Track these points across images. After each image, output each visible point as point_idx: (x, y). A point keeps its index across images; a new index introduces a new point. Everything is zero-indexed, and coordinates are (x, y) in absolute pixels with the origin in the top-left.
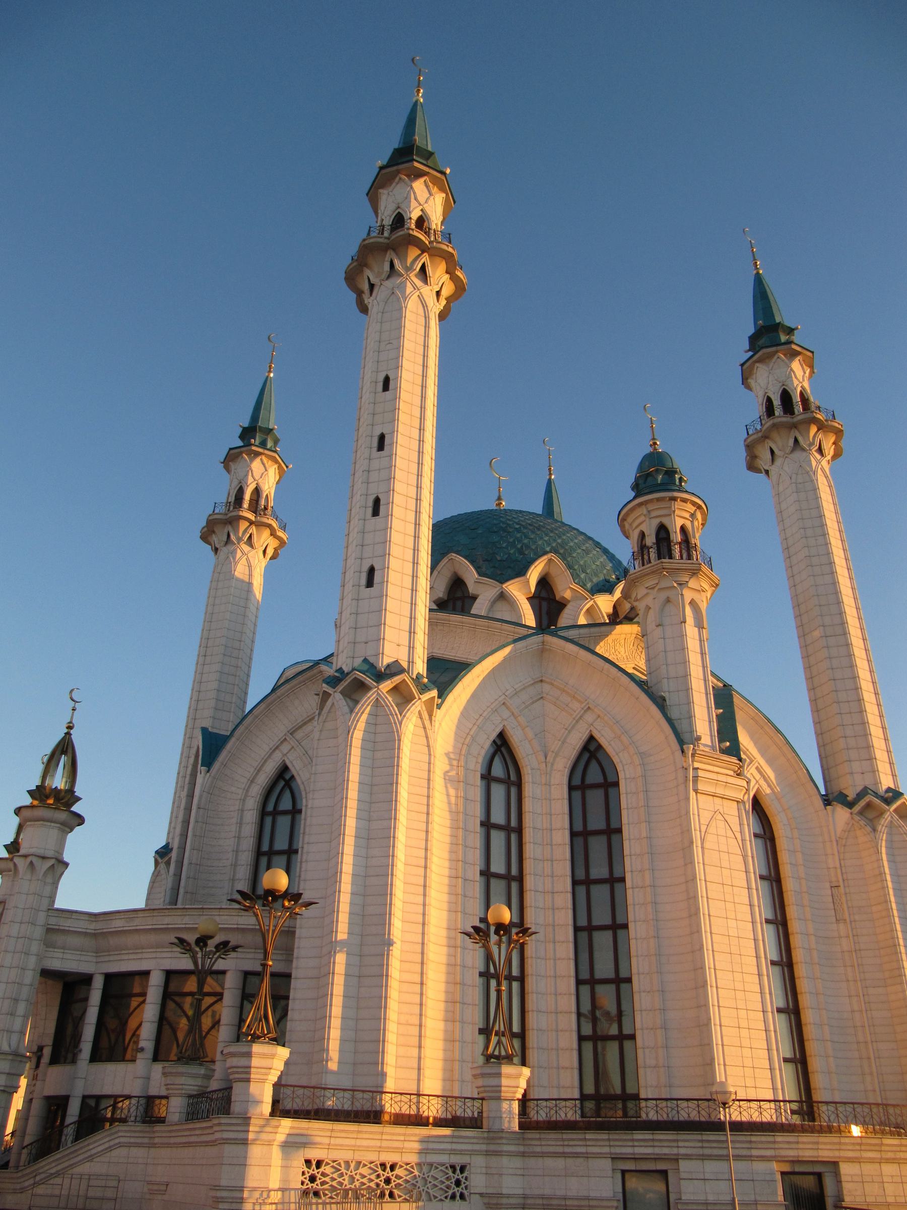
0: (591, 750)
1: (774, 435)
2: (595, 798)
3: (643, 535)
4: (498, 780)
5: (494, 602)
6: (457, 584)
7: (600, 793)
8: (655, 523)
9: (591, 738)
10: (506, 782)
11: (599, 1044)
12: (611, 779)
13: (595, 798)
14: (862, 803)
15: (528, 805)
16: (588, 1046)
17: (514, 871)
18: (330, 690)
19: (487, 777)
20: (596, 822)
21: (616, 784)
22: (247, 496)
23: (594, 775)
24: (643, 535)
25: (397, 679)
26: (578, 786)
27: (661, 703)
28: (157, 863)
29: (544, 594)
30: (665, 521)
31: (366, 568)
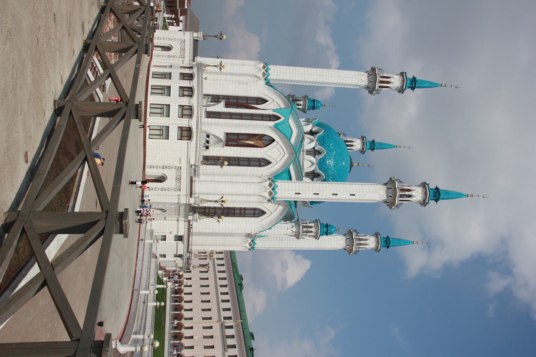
0: (263, 213)
3: (312, 227)
8: (313, 231)
13: (252, 212)
18: (272, 188)
20: (247, 212)
21: (254, 217)
23: (257, 212)
24: (312, 227)
26: (255, 209)
30: (312, 234)
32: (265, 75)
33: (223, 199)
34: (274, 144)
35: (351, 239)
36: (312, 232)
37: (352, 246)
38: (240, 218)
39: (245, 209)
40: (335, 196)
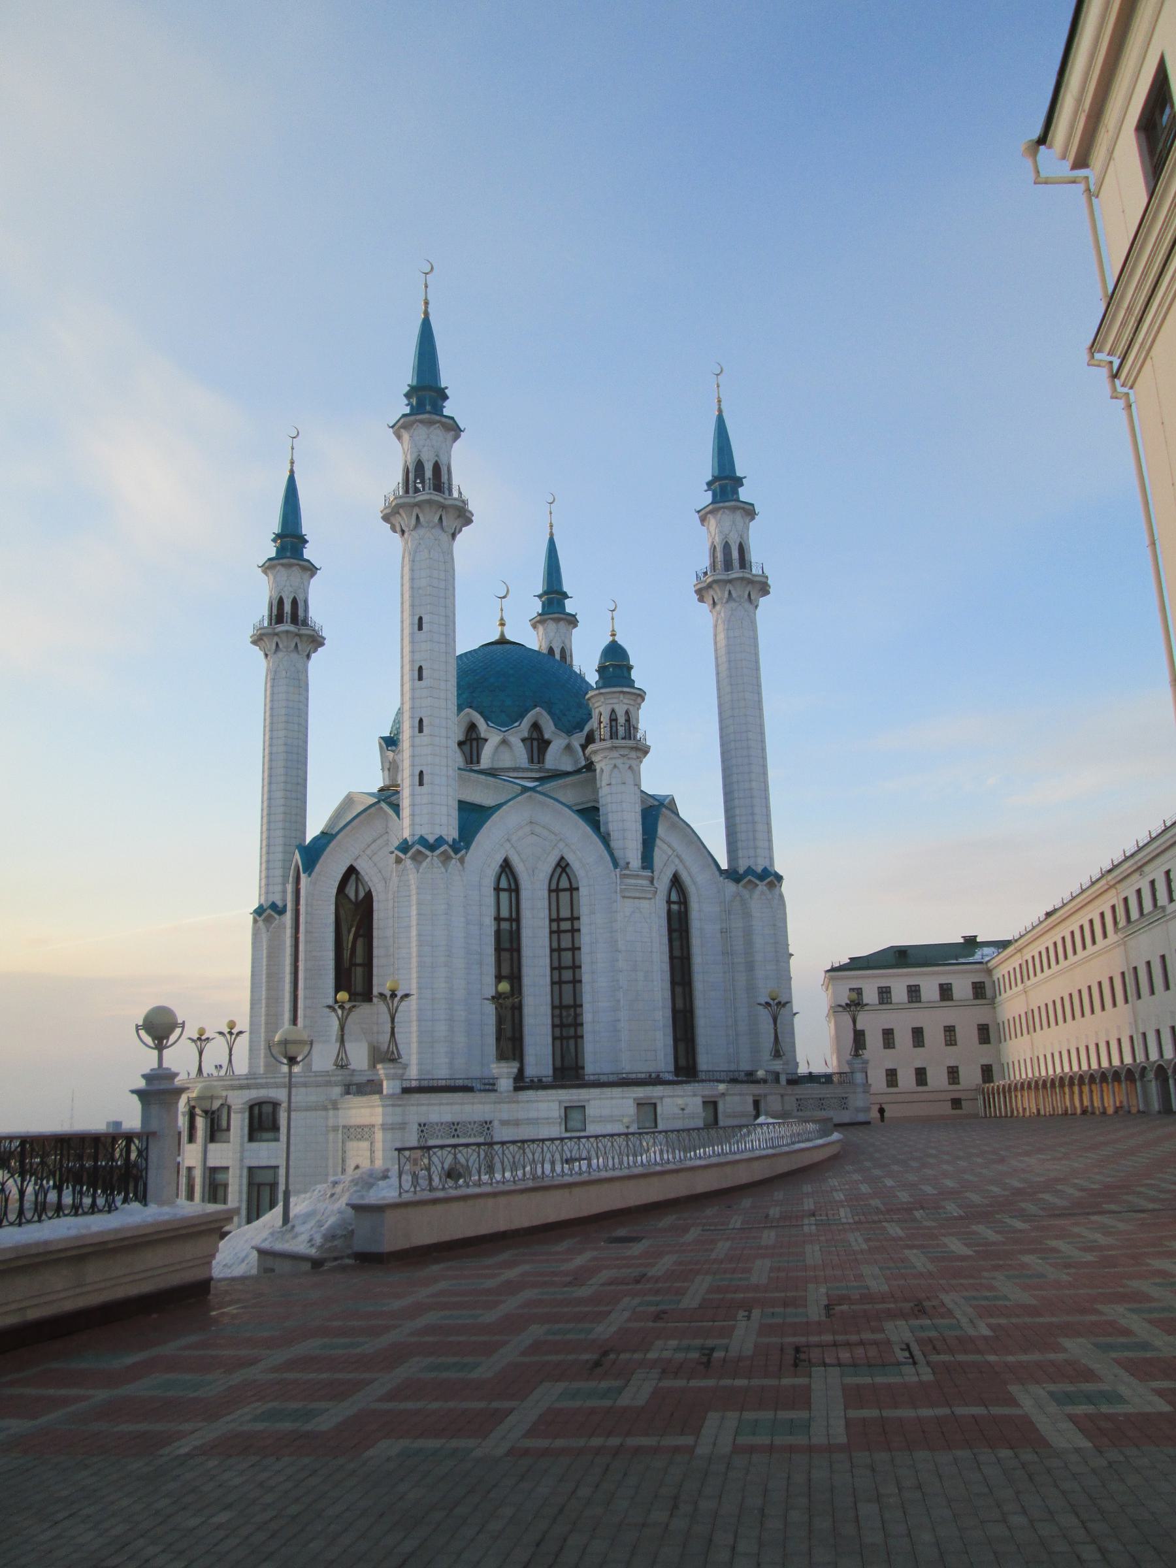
0: (562, 866)
1: (715, 586)
2: (565, 897)
4: (504, 890)
5: (497, 748)
6: (472, 727)
7: (568, 893)
8: (609, 708)
9: (562, 858)
10: (509, 890)
11: (565, 1042)
12: (574, 886)
13: (565, 897)
14: (746, 880)
15: (525, 904)
16: (558, 1043)
17: (515, 946)
19: (497, 889)
20: (565, 913)
22: (287, 608)
23: (564, 883)
25: (442, 849)
26: (554, 891)
27: (605, 840)
28: (255, 921)
29: (535, 735)
30: (617, 708)
31: (417, 773)
32: (270, 916)
33: (388, 994)
34: (361, 866)
35: (711, 592)
36: (613, 711)
37: (730, 581)
38: (584, 930)
39: (555, 920)
40: (425, 673)
